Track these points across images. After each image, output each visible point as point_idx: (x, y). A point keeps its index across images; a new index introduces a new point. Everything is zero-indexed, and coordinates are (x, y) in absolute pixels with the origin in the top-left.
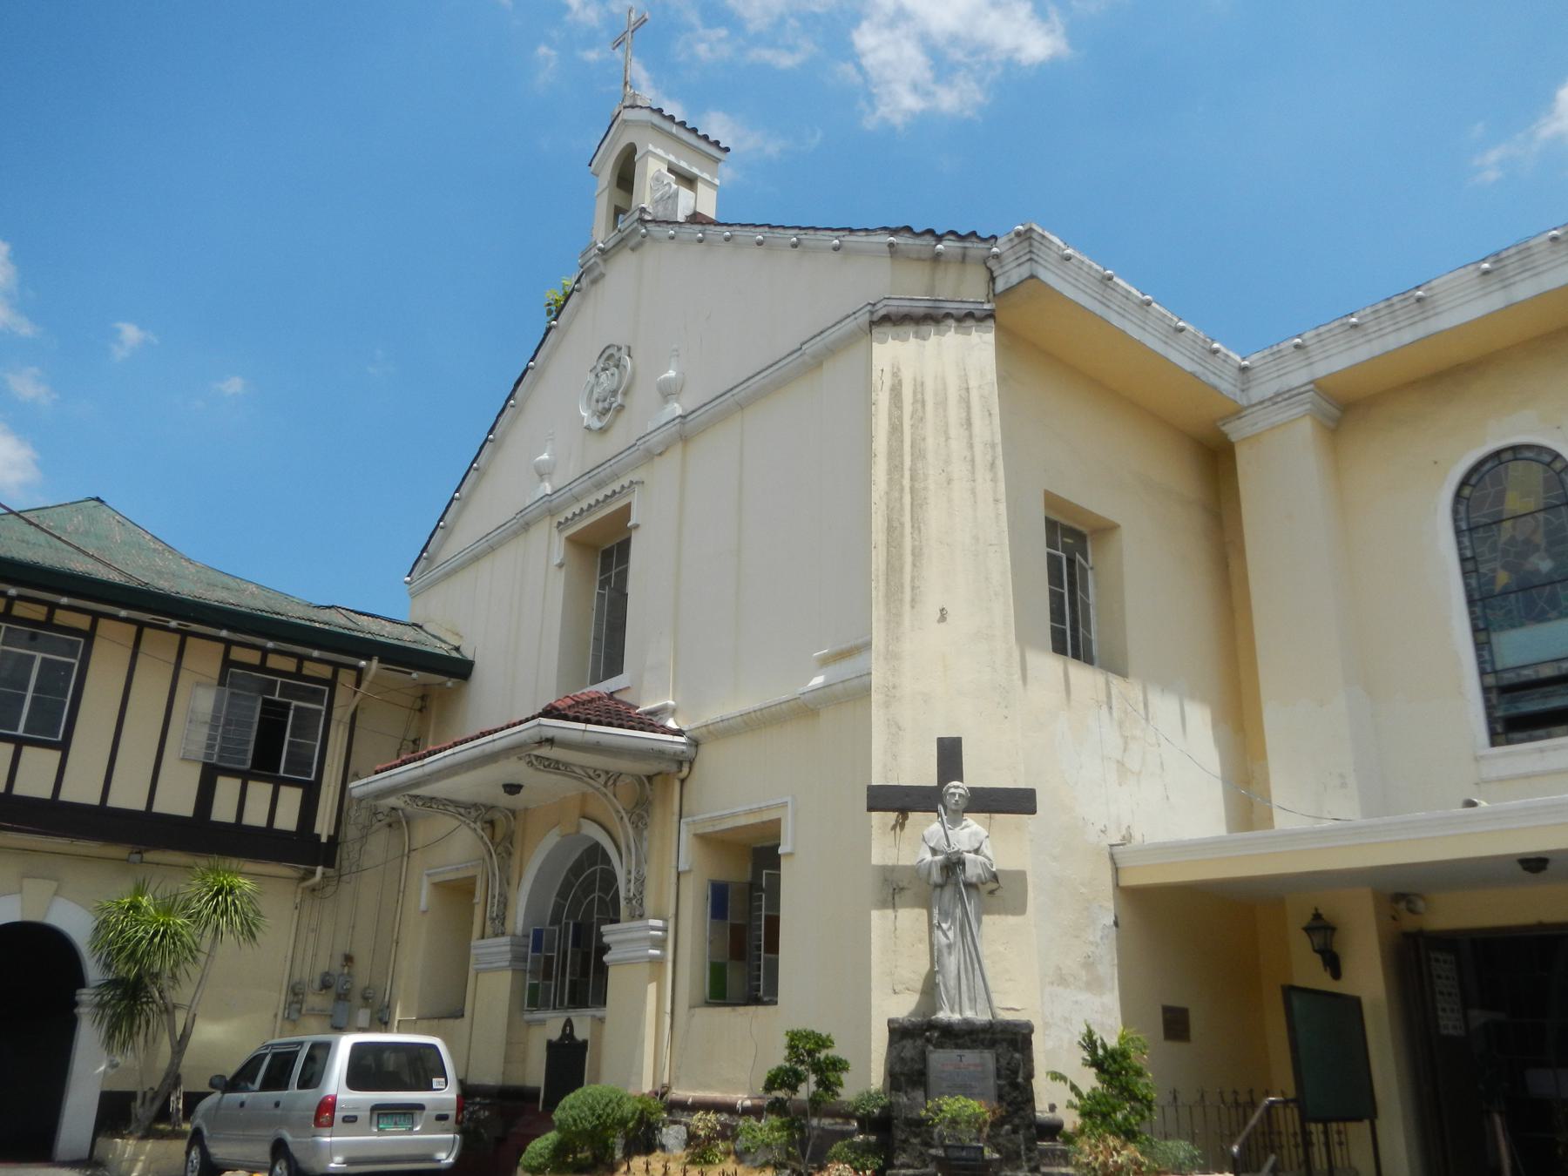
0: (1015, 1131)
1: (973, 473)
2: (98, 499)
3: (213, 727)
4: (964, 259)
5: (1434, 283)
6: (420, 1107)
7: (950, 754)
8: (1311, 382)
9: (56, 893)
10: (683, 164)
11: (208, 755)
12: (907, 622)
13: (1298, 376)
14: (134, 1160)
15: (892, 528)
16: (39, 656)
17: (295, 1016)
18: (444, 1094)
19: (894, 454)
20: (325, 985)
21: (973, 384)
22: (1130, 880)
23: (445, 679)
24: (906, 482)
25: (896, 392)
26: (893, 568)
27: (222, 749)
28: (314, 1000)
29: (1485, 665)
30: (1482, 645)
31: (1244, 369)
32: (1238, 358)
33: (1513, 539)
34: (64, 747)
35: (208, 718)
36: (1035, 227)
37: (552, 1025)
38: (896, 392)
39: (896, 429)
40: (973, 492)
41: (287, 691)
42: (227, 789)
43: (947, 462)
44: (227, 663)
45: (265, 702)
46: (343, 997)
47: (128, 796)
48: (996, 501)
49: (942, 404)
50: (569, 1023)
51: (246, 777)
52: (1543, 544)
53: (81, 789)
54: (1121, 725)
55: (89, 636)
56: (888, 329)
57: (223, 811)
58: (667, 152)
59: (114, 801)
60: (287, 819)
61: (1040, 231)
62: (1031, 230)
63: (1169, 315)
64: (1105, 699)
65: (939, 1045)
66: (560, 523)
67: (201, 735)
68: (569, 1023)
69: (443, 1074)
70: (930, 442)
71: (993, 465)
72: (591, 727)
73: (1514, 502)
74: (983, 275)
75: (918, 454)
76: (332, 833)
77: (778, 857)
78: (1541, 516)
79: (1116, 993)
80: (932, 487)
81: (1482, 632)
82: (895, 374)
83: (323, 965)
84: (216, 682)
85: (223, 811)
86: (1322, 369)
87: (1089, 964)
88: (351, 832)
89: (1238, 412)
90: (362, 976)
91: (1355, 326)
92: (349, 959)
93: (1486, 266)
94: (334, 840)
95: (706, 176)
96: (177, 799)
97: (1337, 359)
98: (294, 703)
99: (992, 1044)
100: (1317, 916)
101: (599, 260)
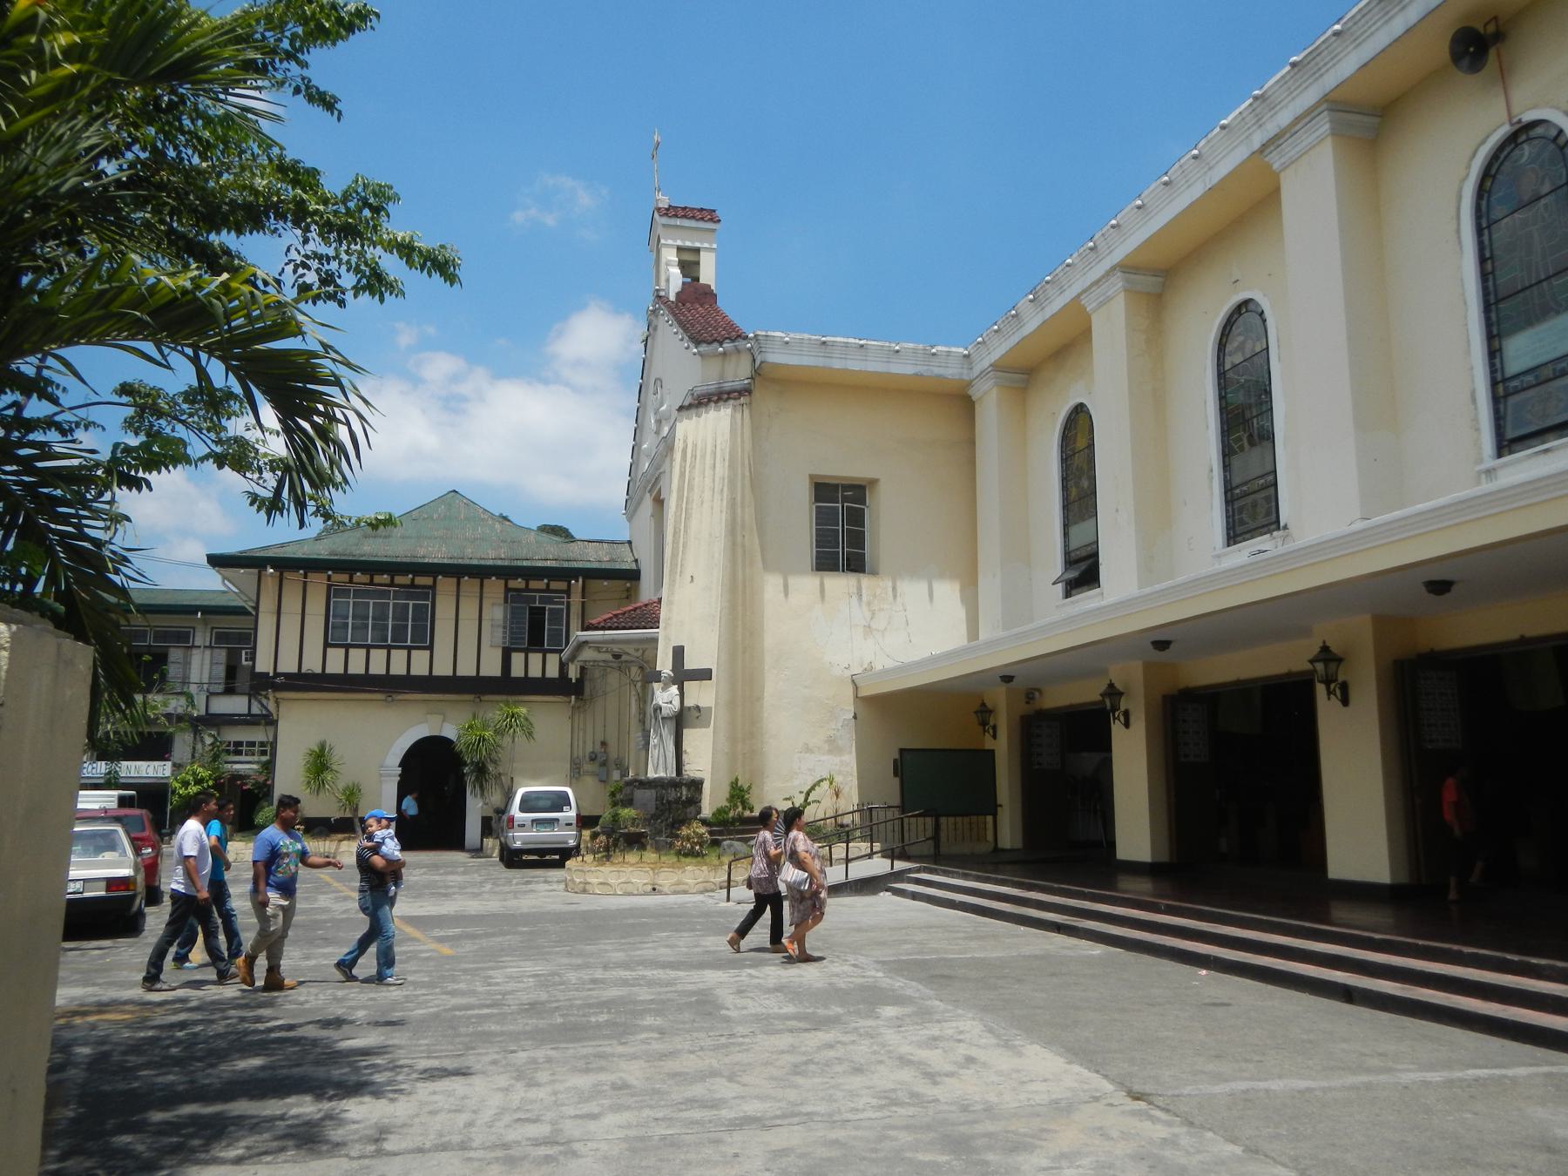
0: (662, 822)
1: (713, 496)
2: (454, 491)
3: (505, 627)
4: (738, 351)
5: (1019, 305)
6: (557, 820)
7: (679, 653)
8: (991, 365)
9: (444, 721)
10: (688, 244)
11: (504, 643)
12: (677, 585)
13: (986, 363)
14: (493, 849)
15: (676, 533)
16: (411, 603)
17: (577, 776)
18: (570, 814)
19: (681, 489)
20: (593, 758)
21: (718, 442)
22: (864, 693)
23: (624, 582)
24: (684, 506)
26: (674, 555)
27: (511, 638)
28: (588, 767)
30: (1066, 534)
31: (965, 356)
32: (961, 350)
34: (431, 648)
35: (501, 623)
36: (759, 333)
39: (682, 474)
40: (712, 508)
41: (542, 600)
42: (517, 659)
43: (703, 492)
44: (507, 589)
45: (531, 608)
46: (604, 764)
47: (466, 669)
48: (721, 511)
49: (703, 456)
51: (526, 651)
53: (443, 669)
54: (869, 604)
55: (433, 587)
56: (684, 413)
57: (517, 671)
58: (675, 240)
59: (460, 673)
60: (553, 671)
61: (764, 333)
62: (756, 336)
63: (887, 344)
64: (855, 591)
65: (639, 788)
67: (499, 633)
69: (570, 804)
70: (697, 479)
71: (722, 490)
72: (607, 632)
74: (749, 358)
75: (691, 488)
76: (578, 676)
79: (854, 754)
80: (695, 506)
82: (685, 441)
83: (589, 748)
84: (502, 601)
85: (517, 671)
86: (995, 355)
87: (831, 741)
89: (969, 384)
90: (613, 754)
91: (996, 331)
92: (604, 744)
93: (1031, 297)
94: (580, 681)
95: (706, 245)
96: (492, 668)
97: (998, 350)
98: (548, 607)
99: (656, 787)
100: (983, 704)
101: (652, 317)
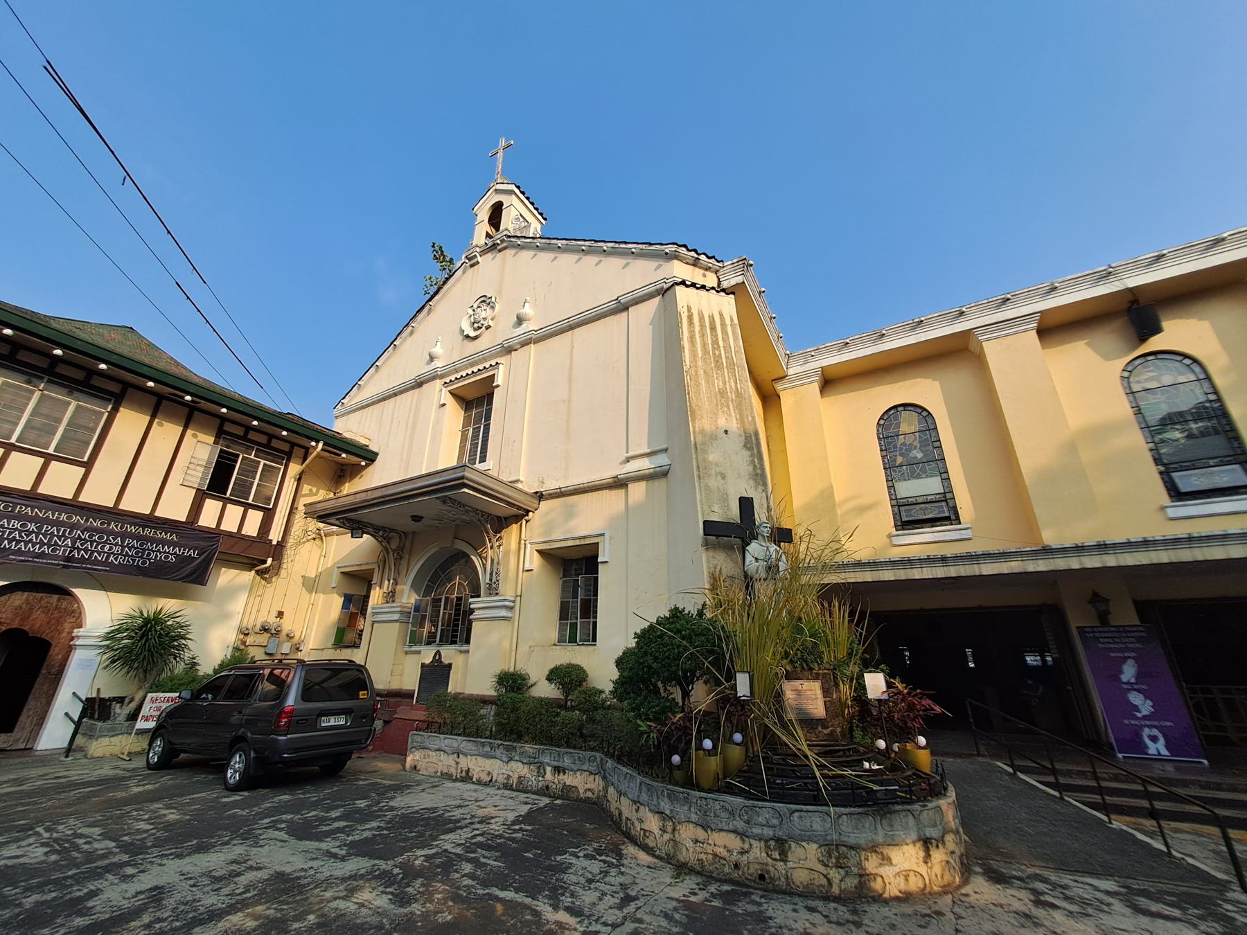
2: (131, 328)
23: (361, 460)
25: (690, 317)
29: (893, 497)
33: (904, 444)
34: (88, 466)
37: (427, 655)
38: (690, 317)
50: (438, 653)
52: (918, 446)
60: (252, 526)
66: (446, 383)
68: (438, 653)
73: (904, 428)
76: (280, 540)
77: (597, 564)
78: (917, 434)
81: (890, 480)
88: (291, 541)
